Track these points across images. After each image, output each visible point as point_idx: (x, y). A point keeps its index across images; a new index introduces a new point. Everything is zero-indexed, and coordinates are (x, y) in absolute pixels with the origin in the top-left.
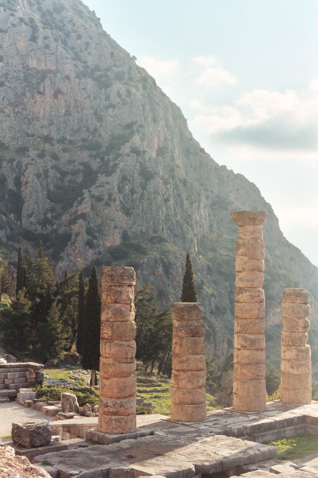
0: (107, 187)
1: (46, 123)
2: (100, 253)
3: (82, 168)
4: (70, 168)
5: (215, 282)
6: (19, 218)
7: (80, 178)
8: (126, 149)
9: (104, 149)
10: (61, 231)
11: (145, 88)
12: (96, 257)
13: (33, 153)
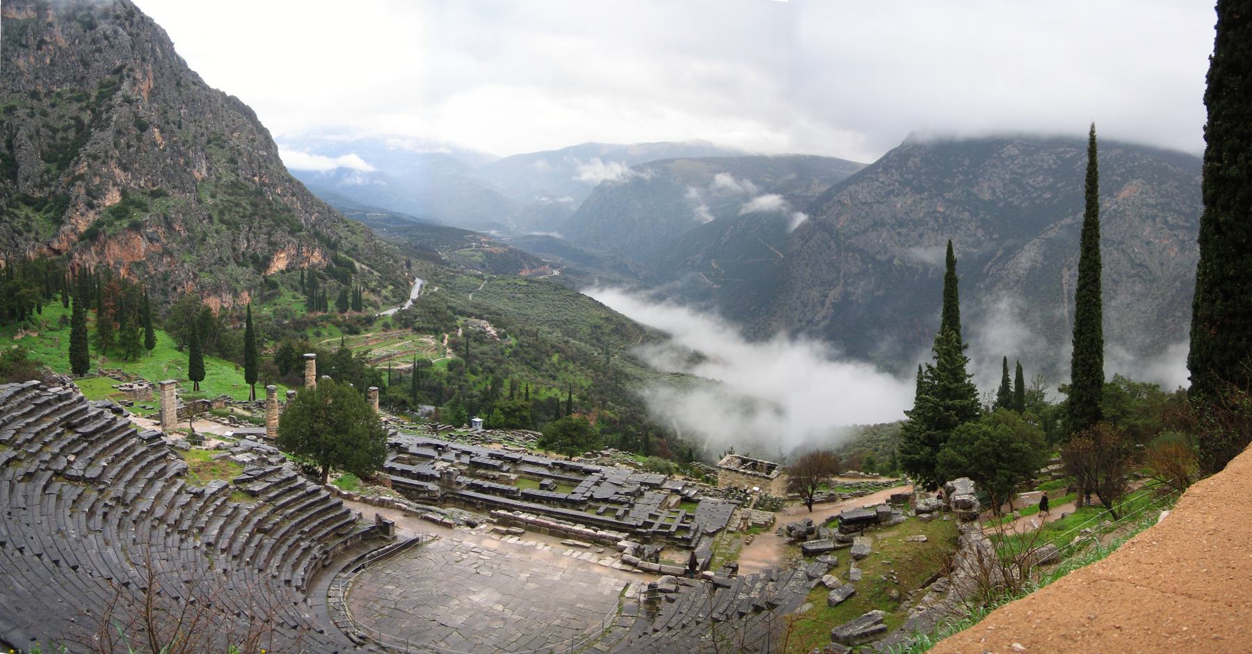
0: (102, 143)
1: (31, 77)
2: (100, 213)
3: (73, 122)
4: (61, 124)
5: (217, 232)
6: (15, 182)
7: (72, 134)
8: (118, 99)
9: (93, 99)
10: (60, 191)
11: (131, 25)
12: (97, 217)
13: (21, 112)
